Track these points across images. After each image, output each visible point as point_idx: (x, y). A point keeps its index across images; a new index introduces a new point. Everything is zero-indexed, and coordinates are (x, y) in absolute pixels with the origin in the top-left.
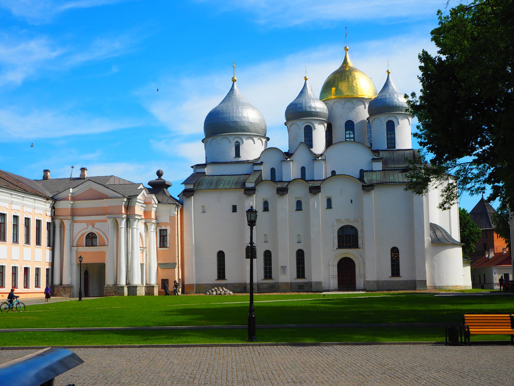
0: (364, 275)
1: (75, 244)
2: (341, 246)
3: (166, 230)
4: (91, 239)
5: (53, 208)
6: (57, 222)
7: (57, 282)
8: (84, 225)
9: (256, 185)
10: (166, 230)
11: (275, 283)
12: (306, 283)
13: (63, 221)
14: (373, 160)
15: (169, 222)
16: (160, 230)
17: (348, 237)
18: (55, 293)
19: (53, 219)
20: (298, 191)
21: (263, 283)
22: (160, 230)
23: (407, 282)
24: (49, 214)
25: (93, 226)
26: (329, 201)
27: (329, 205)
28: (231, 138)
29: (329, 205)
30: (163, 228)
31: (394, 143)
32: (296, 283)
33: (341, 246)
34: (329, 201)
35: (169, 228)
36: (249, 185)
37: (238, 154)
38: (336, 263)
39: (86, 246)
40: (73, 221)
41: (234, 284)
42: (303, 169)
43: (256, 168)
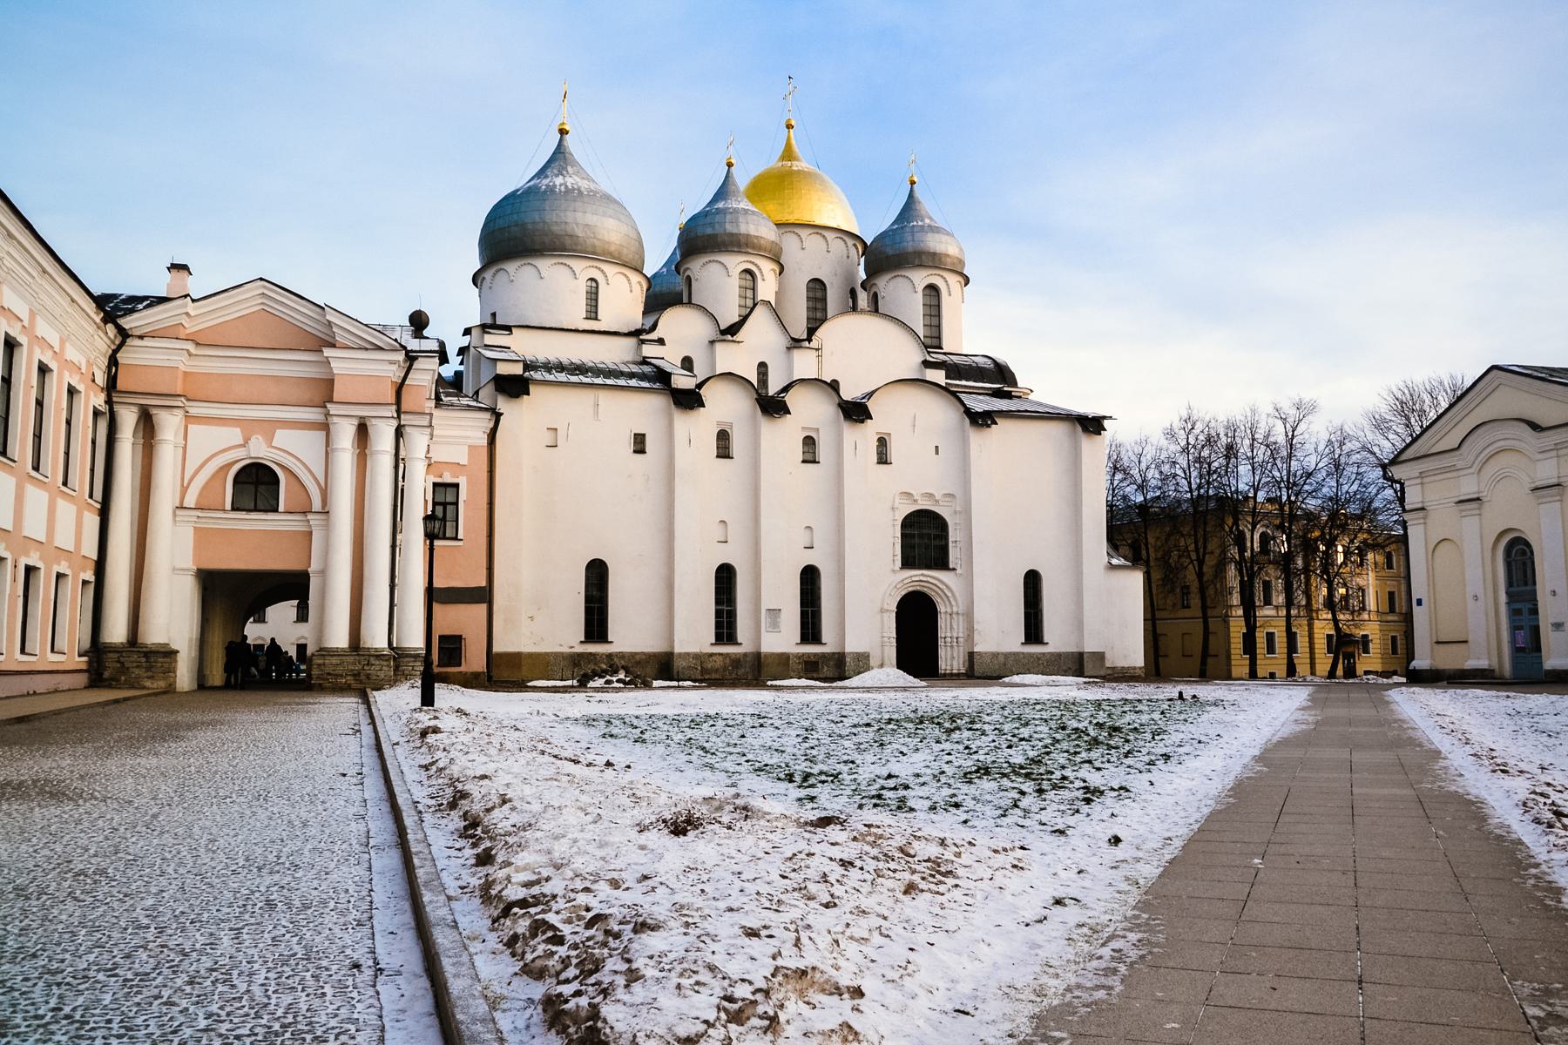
0: (970, 637)
1: (190, 500)
2: (907, 563)
3: (457, 486)
4: (256, 485)
5: (113, 361)
6: (128, 419)
7: (116, 631)
8: (234, 435)
9: (700, 386)
10: (457, 486)
11: (745, 655)
12: (823, 655)
13: (154, 411)
14: (927, 364)
15: (464, 461)
16: (435, 485)
17: (925, 539)
18: (106, 674)
19: (109, 402)
20: (809, 410)
21: (711, 655)
22: (435, 485)
23: (1059, 655)
24: (101, 379)
25: (269, 440)
26: (882, 442)
27: (883, 459)
28: (578, 265)
29: (883, 459)
30: (448, 479)
31: (939, 338)
32: (800, 656)
33: (907, 563)
34: (882, 442)
35: (463, 482)
36: (682, 381)
37: (593, 314)
38: (893, 606)
39: (233, 509)
40: (189, 418)
41: (633, 655)
42: (763, 367)
43: (649, 351)
